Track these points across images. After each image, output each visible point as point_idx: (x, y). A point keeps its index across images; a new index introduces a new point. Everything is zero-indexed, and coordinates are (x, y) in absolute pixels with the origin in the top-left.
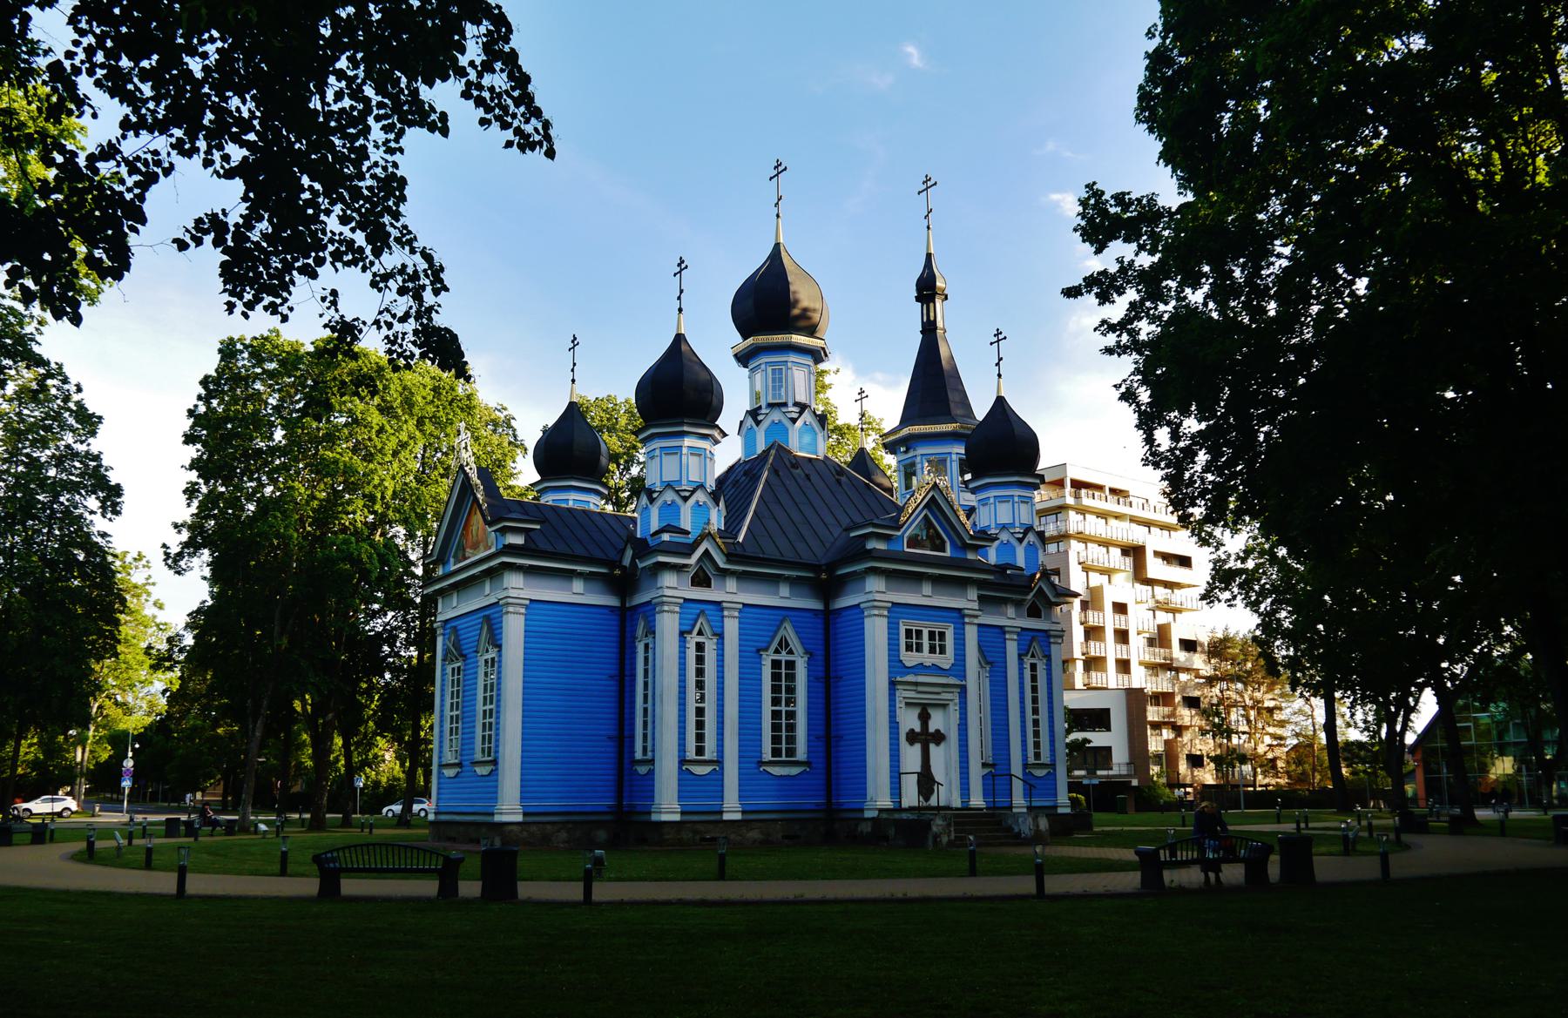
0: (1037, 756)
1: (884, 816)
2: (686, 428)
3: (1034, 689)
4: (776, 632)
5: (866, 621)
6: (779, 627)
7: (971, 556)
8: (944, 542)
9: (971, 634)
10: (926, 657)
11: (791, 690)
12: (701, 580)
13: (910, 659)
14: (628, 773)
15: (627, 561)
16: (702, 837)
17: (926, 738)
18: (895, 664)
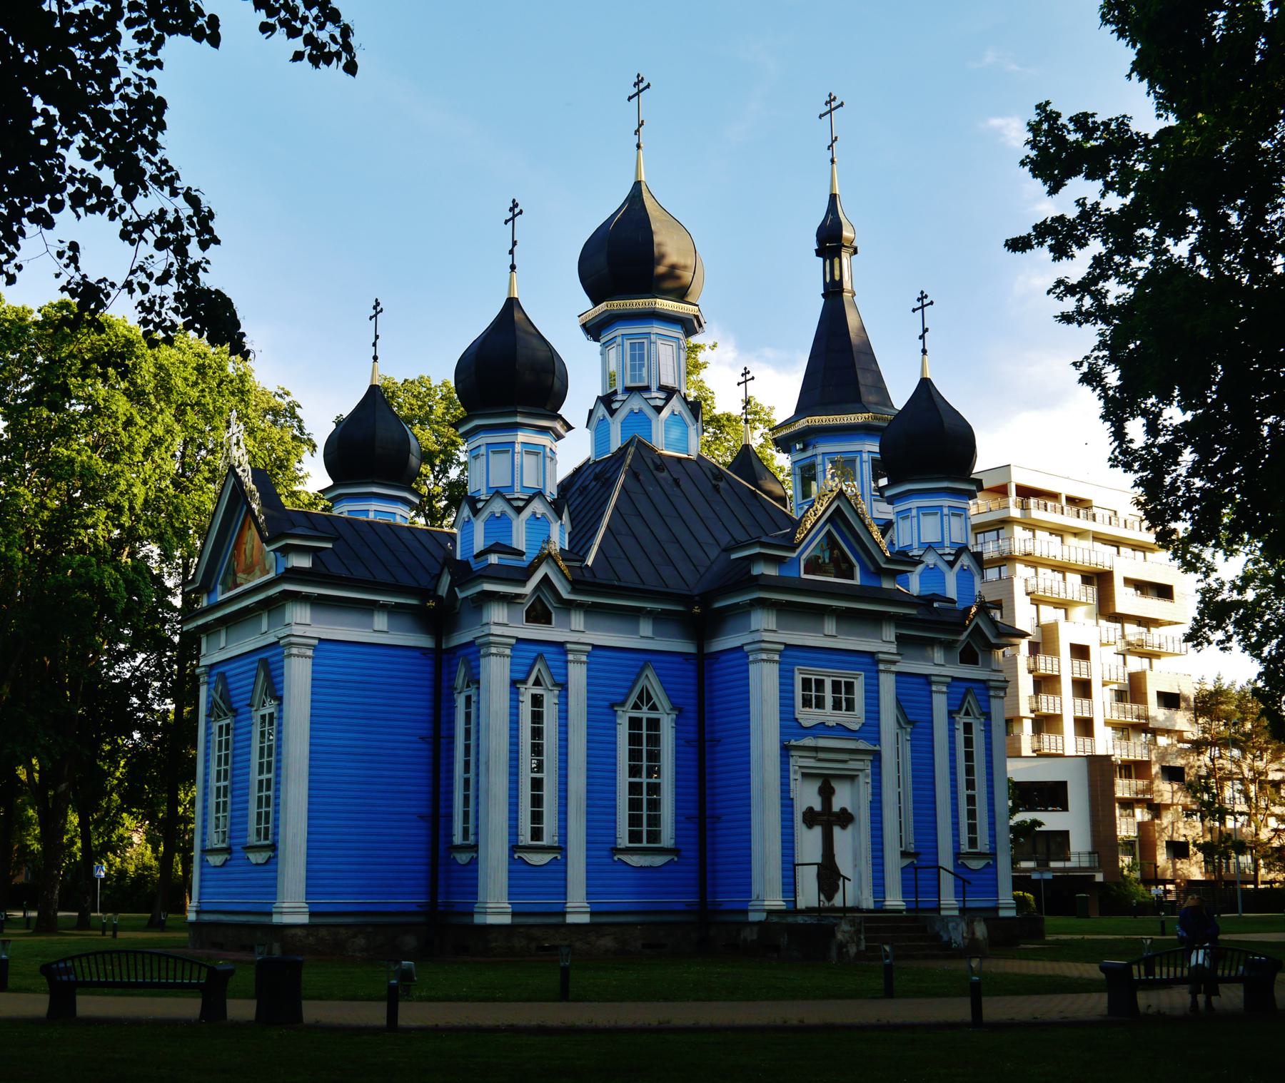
0: (973, 842)
1: (775, 919)
2: (519, 419)
3: (969, 756)
4: (635, 682)
5: (751, 667)
6: (639, 675)
7: (887, 584)
8: (852, 567)
9: (887, 685)
10: (829, 715)
11: (654, 756)
12: (538, 614)
13: (808, 717)
14: (447, 866)
15: (443, 590)
16: (538, 944)
17: (828, 820)
18: (789, 724)
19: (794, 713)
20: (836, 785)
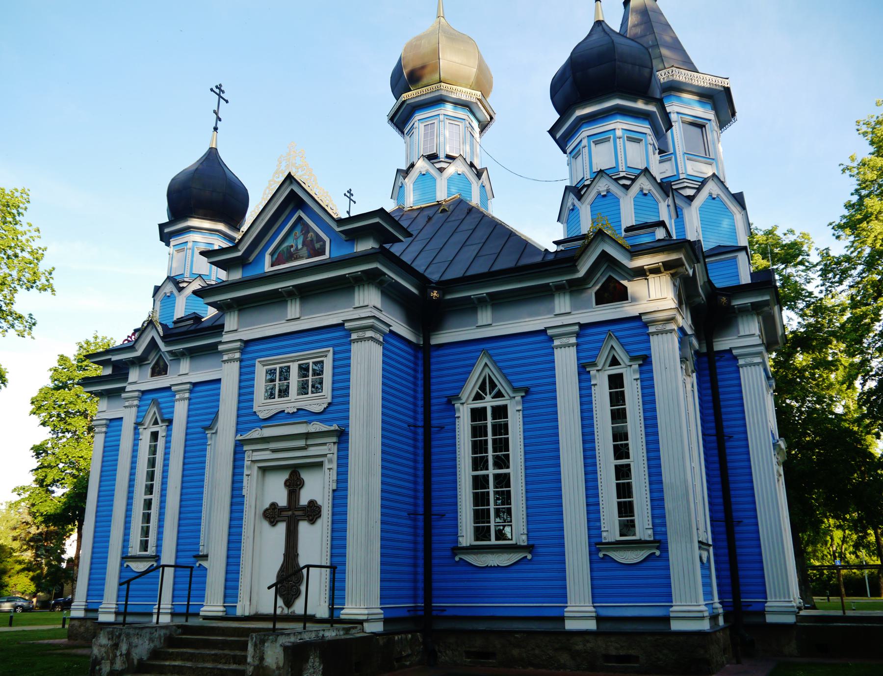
10: (293, 401)
17: (292, 515)
19: (252, 407)
20: (305, 476)
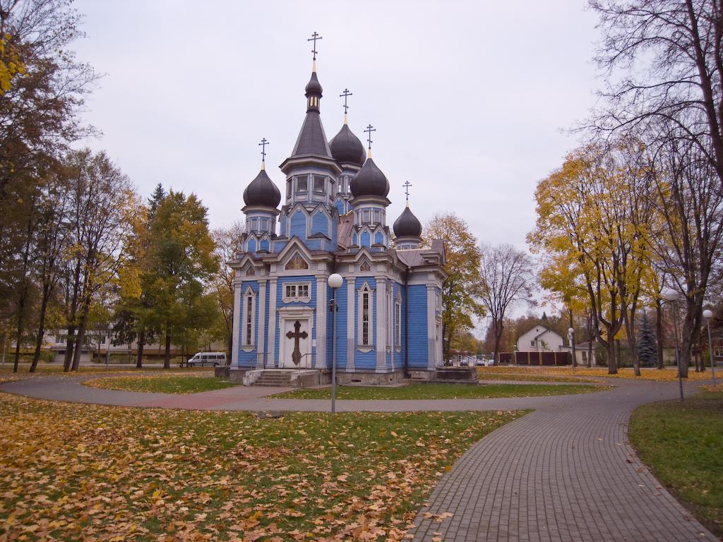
17: (297, 335)
18: (280, 304)
